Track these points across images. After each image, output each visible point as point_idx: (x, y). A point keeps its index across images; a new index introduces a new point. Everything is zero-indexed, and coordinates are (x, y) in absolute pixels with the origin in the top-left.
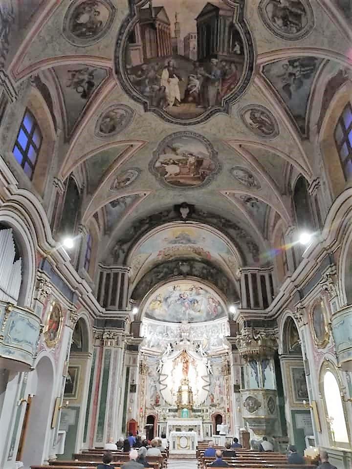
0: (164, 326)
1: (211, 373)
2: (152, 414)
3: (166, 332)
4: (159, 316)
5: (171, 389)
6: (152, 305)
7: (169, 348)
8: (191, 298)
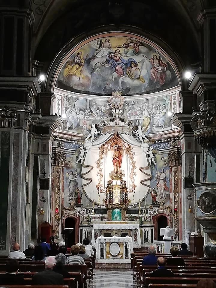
1: (152, 163)
2: (70, 216)
3: (90, 108)
4: (78, 85)
6: (67, 69)
7: (94, 130)
8: (127, 58)
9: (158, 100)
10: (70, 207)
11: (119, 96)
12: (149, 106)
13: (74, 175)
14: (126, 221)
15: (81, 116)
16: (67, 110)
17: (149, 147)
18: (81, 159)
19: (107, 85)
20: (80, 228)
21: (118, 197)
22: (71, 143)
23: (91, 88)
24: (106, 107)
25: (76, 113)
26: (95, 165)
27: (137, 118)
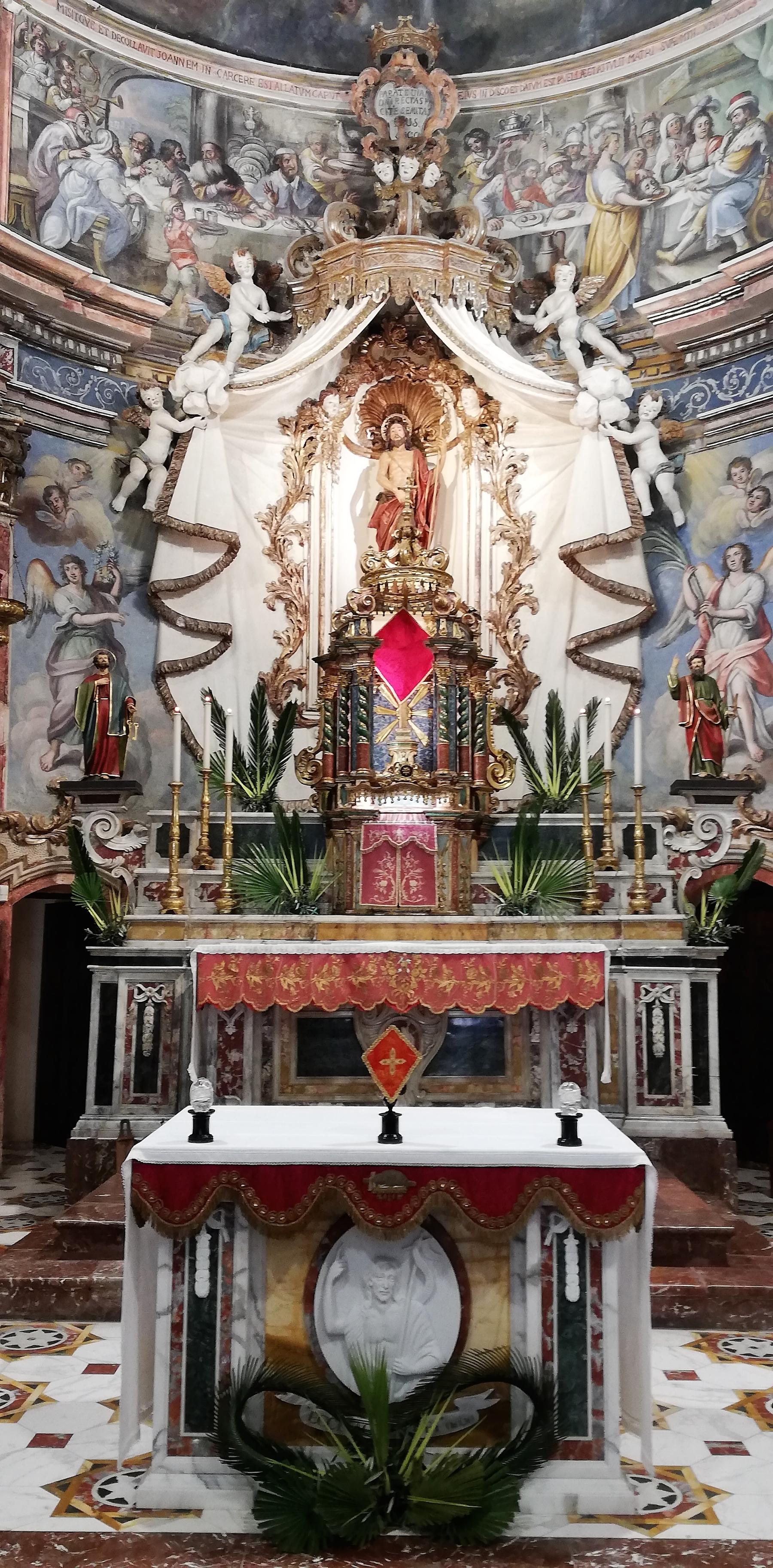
0: (197, 94)
3: (221, 153)
5: (267, 668)
7: (248, 301)
9: (697, 73)
10: (56, 812)
11: (425, 73)
12: (627, 132)
13: (96, 591)
14: (485, 919)
15: (153, 191)
16: (45, 124)
17: (633, 403)
18: (145, 482)
19: (342, 9)
20: (101, 974)
21: (418, 731)
22: (73, 356)
23: (234, 21)
24: (336, 157)
25: (122, 167)
26: (254, 542)
27: (544, 220)
